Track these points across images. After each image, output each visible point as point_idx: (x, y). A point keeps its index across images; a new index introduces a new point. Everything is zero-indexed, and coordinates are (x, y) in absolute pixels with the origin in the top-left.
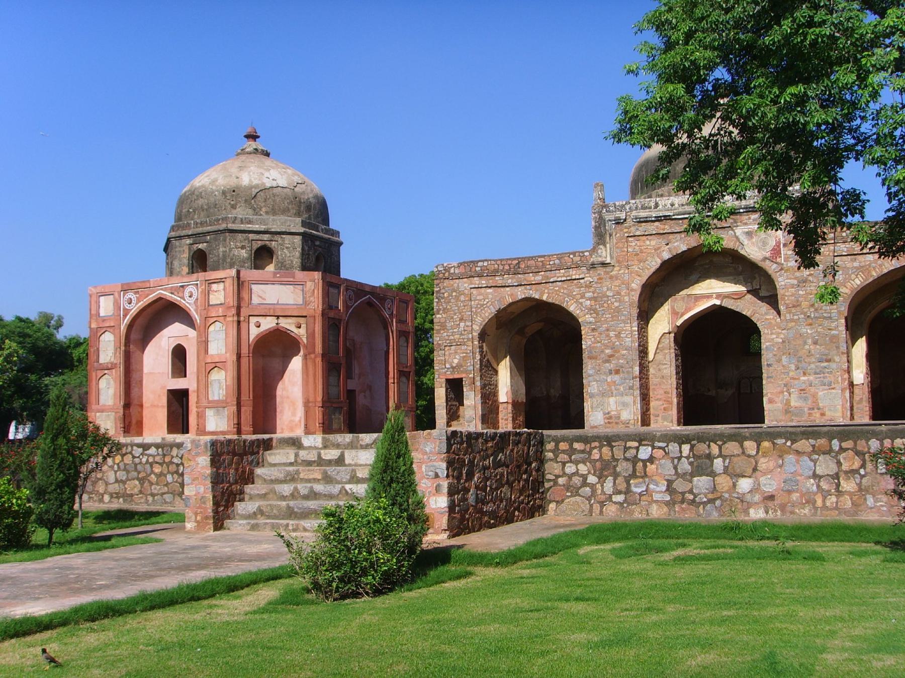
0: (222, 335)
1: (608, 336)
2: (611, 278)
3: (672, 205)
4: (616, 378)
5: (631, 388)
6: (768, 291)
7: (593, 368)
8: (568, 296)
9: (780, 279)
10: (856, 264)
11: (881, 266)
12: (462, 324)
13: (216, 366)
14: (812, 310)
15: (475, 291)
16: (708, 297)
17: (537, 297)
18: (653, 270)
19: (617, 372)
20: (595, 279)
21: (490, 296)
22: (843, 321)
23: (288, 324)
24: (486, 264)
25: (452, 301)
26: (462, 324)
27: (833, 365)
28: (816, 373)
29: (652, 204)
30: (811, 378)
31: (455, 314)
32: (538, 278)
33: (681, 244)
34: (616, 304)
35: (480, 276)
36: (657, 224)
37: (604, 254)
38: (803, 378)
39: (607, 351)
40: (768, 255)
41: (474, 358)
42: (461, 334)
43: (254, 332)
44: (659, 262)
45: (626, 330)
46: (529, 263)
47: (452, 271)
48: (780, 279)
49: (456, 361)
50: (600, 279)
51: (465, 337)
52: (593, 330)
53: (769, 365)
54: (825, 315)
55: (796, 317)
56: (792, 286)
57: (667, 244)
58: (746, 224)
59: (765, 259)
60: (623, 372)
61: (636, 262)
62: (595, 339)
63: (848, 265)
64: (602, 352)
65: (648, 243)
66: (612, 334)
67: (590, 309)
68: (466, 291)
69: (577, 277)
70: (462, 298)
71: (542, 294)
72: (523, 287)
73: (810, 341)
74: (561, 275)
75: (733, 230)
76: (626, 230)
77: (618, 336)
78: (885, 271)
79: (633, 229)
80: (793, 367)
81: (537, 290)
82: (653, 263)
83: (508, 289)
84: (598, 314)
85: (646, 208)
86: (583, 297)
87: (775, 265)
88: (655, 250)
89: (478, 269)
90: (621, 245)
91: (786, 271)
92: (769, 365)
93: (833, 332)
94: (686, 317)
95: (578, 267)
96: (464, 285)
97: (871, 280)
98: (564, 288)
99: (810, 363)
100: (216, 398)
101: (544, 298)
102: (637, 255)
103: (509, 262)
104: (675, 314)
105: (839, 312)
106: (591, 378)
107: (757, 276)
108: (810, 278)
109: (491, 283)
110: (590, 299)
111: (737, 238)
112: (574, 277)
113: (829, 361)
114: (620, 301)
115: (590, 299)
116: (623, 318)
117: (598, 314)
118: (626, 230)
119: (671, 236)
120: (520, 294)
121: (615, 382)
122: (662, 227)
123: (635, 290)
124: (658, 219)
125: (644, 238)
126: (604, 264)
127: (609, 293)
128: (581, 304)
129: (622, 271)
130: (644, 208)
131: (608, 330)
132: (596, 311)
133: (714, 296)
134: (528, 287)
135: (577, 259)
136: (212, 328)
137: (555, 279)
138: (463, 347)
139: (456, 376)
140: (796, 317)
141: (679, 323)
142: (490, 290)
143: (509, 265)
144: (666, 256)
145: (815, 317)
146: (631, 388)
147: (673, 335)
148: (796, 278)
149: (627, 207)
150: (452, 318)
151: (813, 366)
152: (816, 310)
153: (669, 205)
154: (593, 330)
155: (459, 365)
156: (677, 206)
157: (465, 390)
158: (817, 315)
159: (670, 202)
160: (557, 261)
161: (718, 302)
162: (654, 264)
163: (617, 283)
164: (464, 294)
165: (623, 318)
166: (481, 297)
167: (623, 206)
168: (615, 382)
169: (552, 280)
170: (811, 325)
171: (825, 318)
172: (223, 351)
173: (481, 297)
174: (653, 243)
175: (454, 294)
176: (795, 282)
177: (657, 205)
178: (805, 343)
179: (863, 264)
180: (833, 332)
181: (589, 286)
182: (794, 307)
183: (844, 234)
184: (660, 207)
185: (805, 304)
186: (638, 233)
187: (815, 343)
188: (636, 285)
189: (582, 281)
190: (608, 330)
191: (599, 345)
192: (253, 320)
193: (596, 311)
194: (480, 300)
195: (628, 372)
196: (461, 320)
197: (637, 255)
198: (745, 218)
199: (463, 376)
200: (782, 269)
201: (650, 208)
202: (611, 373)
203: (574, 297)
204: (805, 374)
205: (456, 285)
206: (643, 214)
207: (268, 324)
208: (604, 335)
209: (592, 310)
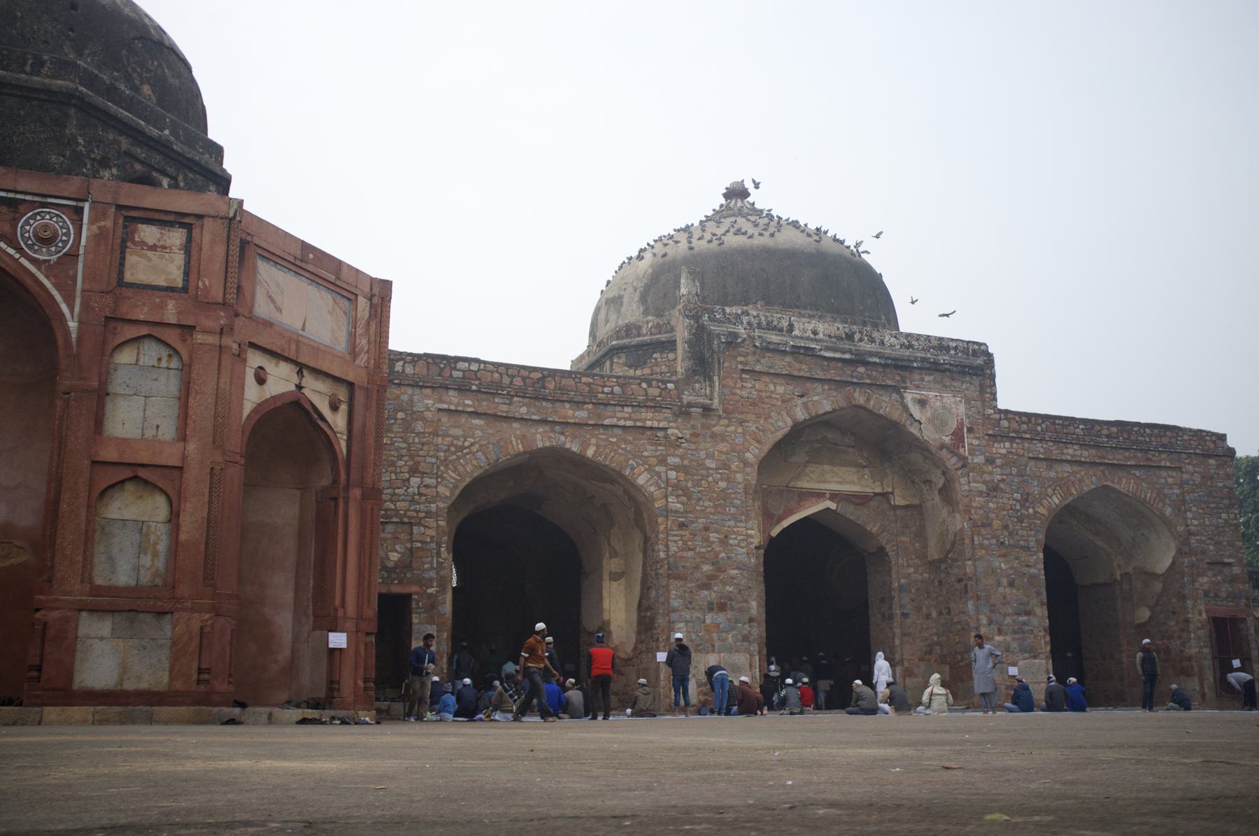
0: (169, 384)
1: (706, 539)
2: (713, 436)
3: (815, 333)
4: (721, 618)
5: (746, 638)
6: (904, 498)
7: (680, 597)
8: (635, 457)
9: (963, 480)
10: (1052, 474)
11: (1081, 481)
12: (415, 481)
13: (138, 474)
14: (1006, 533)
15: (444, 420)
16: (820, 495)
17: (575, 449)
18: (780, 435)
19: (722, 607)
20: (687, 433)
21: (478, 433)
22: (1041, 555)
23: (317, 393)
24: (474, 367)
25: (396, 428)
26: (415, 481)
27: (1035, 621)
28: (1015, 632)
29: (785, 324)
30: (1008, 638)
31: (400, 457)
32: (581, 414)
33: (824, 402)
34: (722, 484)
35: (462, 389)
36: (788, 359)
37: (712, 393)
38: (997, 638)
39: (706, 568)
40: (947, 440)
41: (439, 554)
42: (413, 501)
43: (253, 395)
44: (790, 423)
45: (737, 533)
46: (564, 381)
47: (398, 366)
48: (963, 480)
49: (394, 556)
50: (696, 435)
51: (422, 507)
52: (682, 526)
53: (905, 615)
54: (1022, 543)
55: (986, 542)
56: (981, 493)
57: (801, 396)
58: (917, 387)
59: (942, 446)
60: (732, 609)
61: (753, 417)
62: (685, 543)
63: (1045, 474)
64: (697, 567)
65: (772, 387)
66: (713, 537)
67: (676, 487)
68: (429, 415)
69: (656, 424)
70: (419, 426)
71: (585, 445)
72: (547, 428)
73: (1004, 581)
74: (622, 416)
75: (899, 392)
76: (740, 359)
77: (724, 541)
78: (1086, 489)
79: (750, 358)
80: (984, 621)
81: (574, 437)
82: (780, 424)
83: (516, 425)
84: (690, 498)
85: (774, 328)
86: (662, 461)
87: (954, 460)
88: (783, 401)
89: (456, 374)
90: (731, 383)
91: (973, 469)
92: (905, 615)
93: (1033, 570)
94: (786, 523)
95: (657, 407)
96: (426, 402)
97: (1071, 499)
98: (626, 442)
99: (1006, 615)
100: (123, 578)
101: (590, 453)
102: (754, 404)
103: (525, 374)
104: (769, 518)
105: (1037, 541)
106: (674, 616)
107: (888, 471)
108: (1002, 485)
109: (484, 406)
110: (676, 468)
111: (905, 408)
112: (649, 424)
113: (1028, 613)
114: (728, 480)
115: (676, 468)
116: (733, 510)
117: (690, 498)
118: (740, 359)
119: (808, 385)
120: (542, 439)
121: (718, 626)
122: (797, 365)
123: (751, 465)
124: (796, 351)
125: (766, 379)
126: (707, 410)
127: (710, 464)
128: (658, 474)
129: (732, 428)
130: (770, 327)
131: (706, 529)
132: (687, 493)
133: (828, 496)
134: (557, 428)
135: (654, 392)
136: (126, 357)
137: (614, 421)
138: (416, 529)
139: (396, 589)
140: (986, 542)
141: (775, 532)
142: (477, 422)
143: (524, 379)
144: (801, 415)
145: (1010, 546)
146: (746, 638)
147: (762, 551)
148: (984, 482)
149: (745, 319)
150: (393, 464)
151: (1008, 620)
152: (1011, 534)
153: (809, 334)
154: (682, 526)
155: (406, 565)
156: (821, 336)
157: (415, 620)
158: (1012, 542)
159: (811, 327)
160: (617, 389)
161: (833, 506)
162: (783, 425)
163: (723, 447)
164: (423, 419)
165: (733, 510)
166: (459, 432)
167: (738, 316)
168: (718, 626)
169: (606, 422)
170: (1004, 556)
171: (1022, 548)
172: (168, 431)
173: (459, 432)
174: (780, 389)
175: (400, 415)
176: (983, 488)
177: (791, 328)
178: (999, 584)
179: (1060, 475)
180: (1033, 570)
181: (676, 443)
182: (984, 525)
183: (1039, 428)
184: (796, 332)
185: (997, 524)
186: (758, 368)
187: (1011, 584)
188: (754, 454)
189: (660, 434)
190: (706, 529)
191: (690, 554)
192: (255, 359)
193: (687, 493)
194: (457, 438)
195: (741, 610)
196: (414, 471)
197: (754, 404)
198: (917, 377)
199: (414, 589)
200: (964, 466)
201: (781, 330)
202: (711, 609)
203: (645, 460)
204: (1000, 632)
205: (405, 398)
206: (774, 338)
207: (281, 380)
208: (698, 538)
209: (680, 490)
